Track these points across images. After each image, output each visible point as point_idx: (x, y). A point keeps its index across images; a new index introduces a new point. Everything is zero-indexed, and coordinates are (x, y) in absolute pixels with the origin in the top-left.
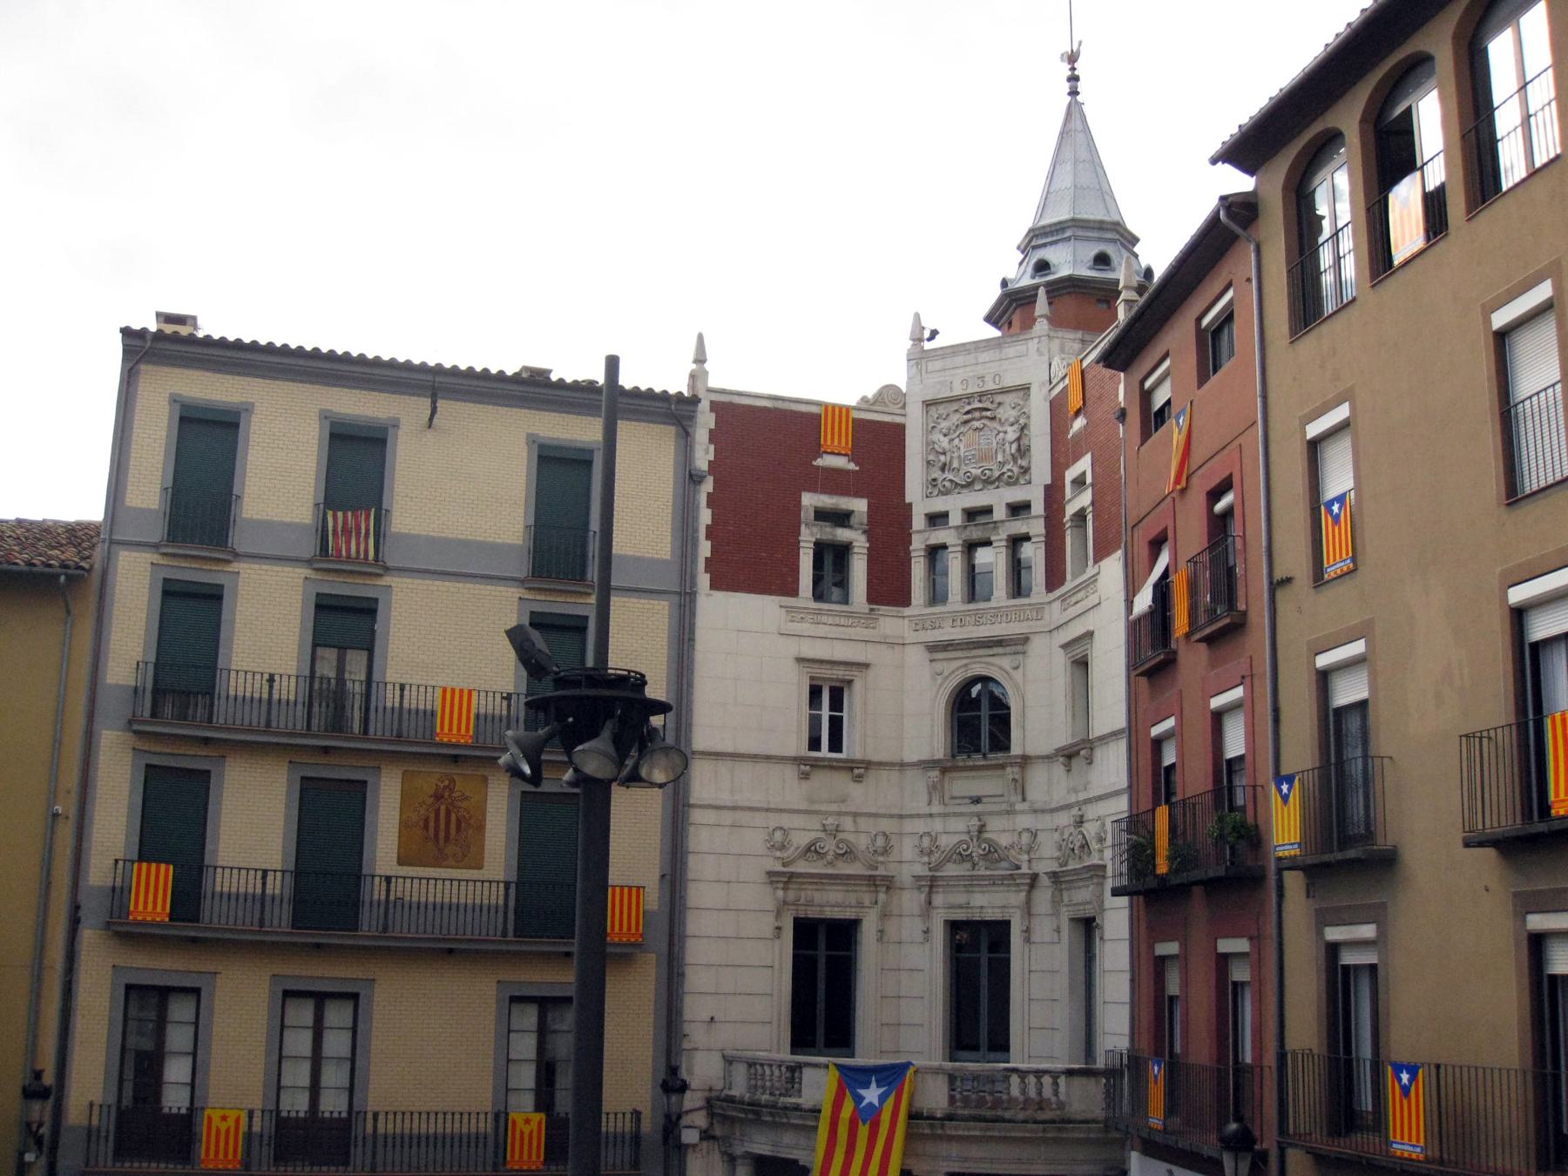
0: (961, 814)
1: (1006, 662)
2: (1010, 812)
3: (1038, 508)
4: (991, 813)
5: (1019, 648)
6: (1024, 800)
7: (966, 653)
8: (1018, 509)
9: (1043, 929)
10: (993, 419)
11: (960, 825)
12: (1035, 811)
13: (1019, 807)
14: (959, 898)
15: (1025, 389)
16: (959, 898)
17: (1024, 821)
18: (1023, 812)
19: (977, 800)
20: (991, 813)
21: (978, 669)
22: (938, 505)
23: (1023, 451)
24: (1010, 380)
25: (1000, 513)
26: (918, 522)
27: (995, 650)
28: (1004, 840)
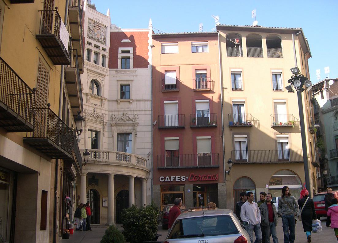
0: (93, 107)
1: (101, 79)
2: (102, 109)
3: (108, 50)
4: (98, 108)
5: (104, 77)
6: (104, 108)
7: (94, 74)
8: (104, 50)
9: (106, 134)
10: (100, 29)
11: (92, 109)
12: (106, 110)
13: (103, 109)
14: (92, 125)
15: (106, 27)
16: (92, 125)
17: (104, 112)
18: (104, 110)
19: (96, 105)
20: (98, 108)
21: (96, 78)
22: (90, 41)
23: (105, 39)
24: (104, 23)
25: (101, 48)
26: (86, 42)
27: (99, 75)
28: (101, 114)
